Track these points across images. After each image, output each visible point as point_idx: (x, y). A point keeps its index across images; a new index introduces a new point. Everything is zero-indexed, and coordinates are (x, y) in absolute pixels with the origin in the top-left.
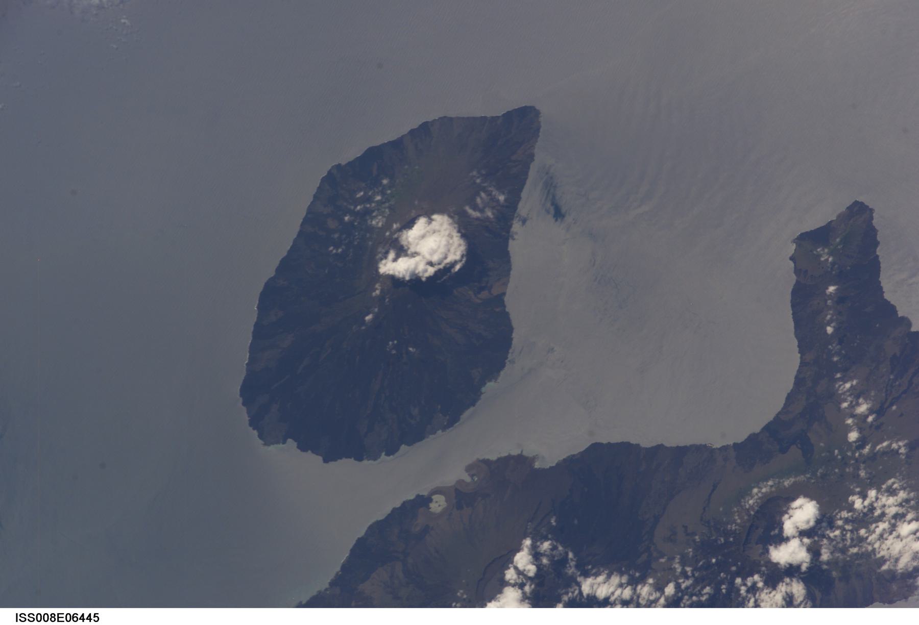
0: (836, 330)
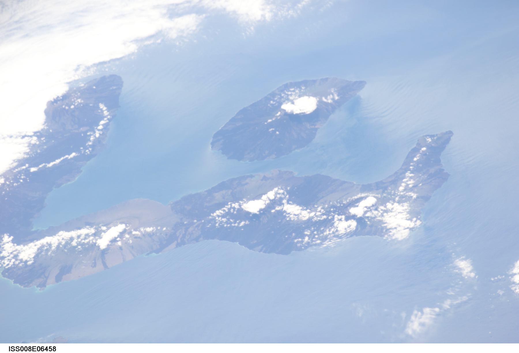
0: (418, 160)
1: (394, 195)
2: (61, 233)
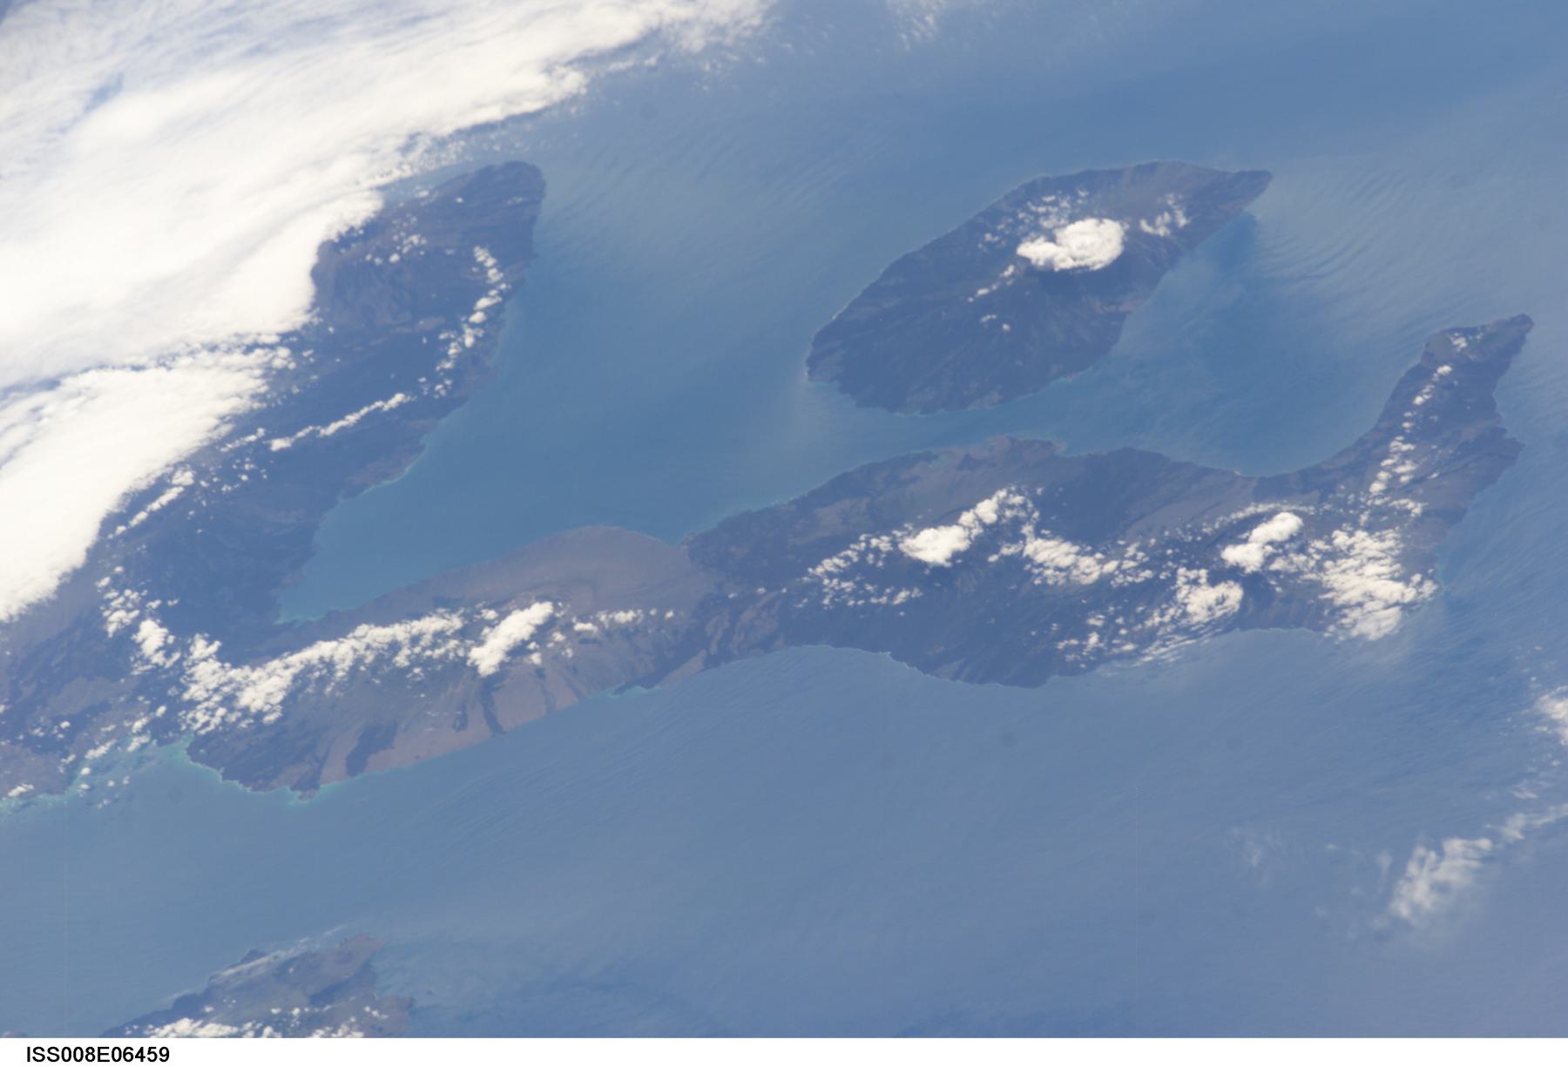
1: (1356, 505)
2: (362, 629)
